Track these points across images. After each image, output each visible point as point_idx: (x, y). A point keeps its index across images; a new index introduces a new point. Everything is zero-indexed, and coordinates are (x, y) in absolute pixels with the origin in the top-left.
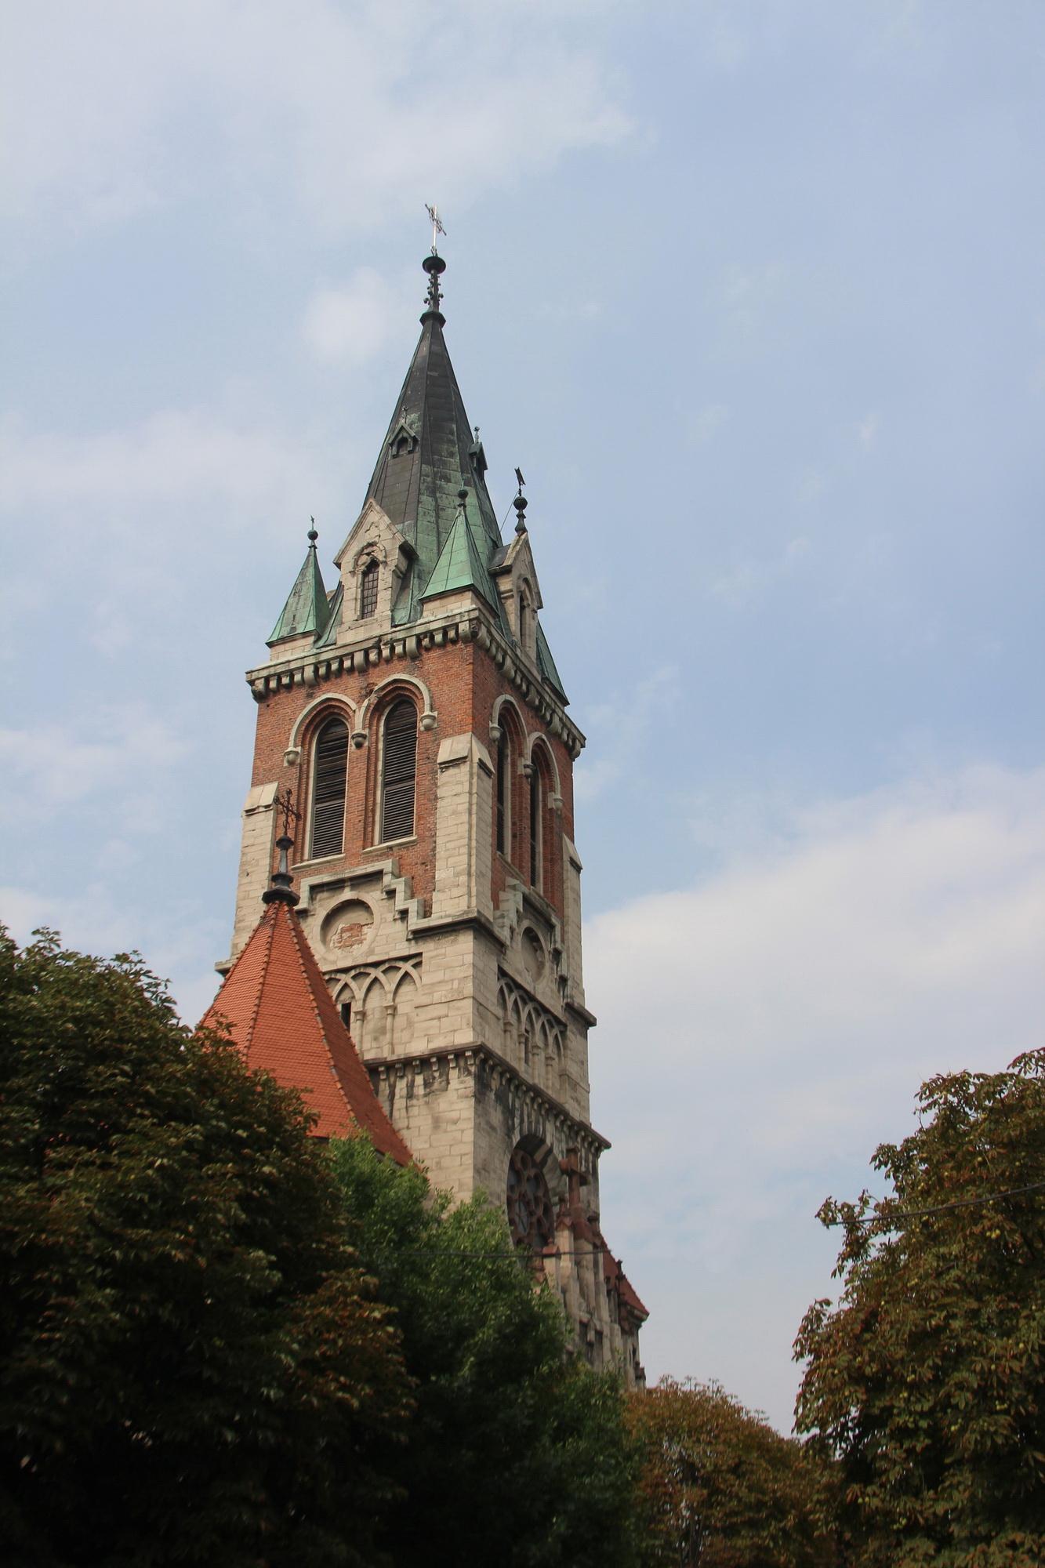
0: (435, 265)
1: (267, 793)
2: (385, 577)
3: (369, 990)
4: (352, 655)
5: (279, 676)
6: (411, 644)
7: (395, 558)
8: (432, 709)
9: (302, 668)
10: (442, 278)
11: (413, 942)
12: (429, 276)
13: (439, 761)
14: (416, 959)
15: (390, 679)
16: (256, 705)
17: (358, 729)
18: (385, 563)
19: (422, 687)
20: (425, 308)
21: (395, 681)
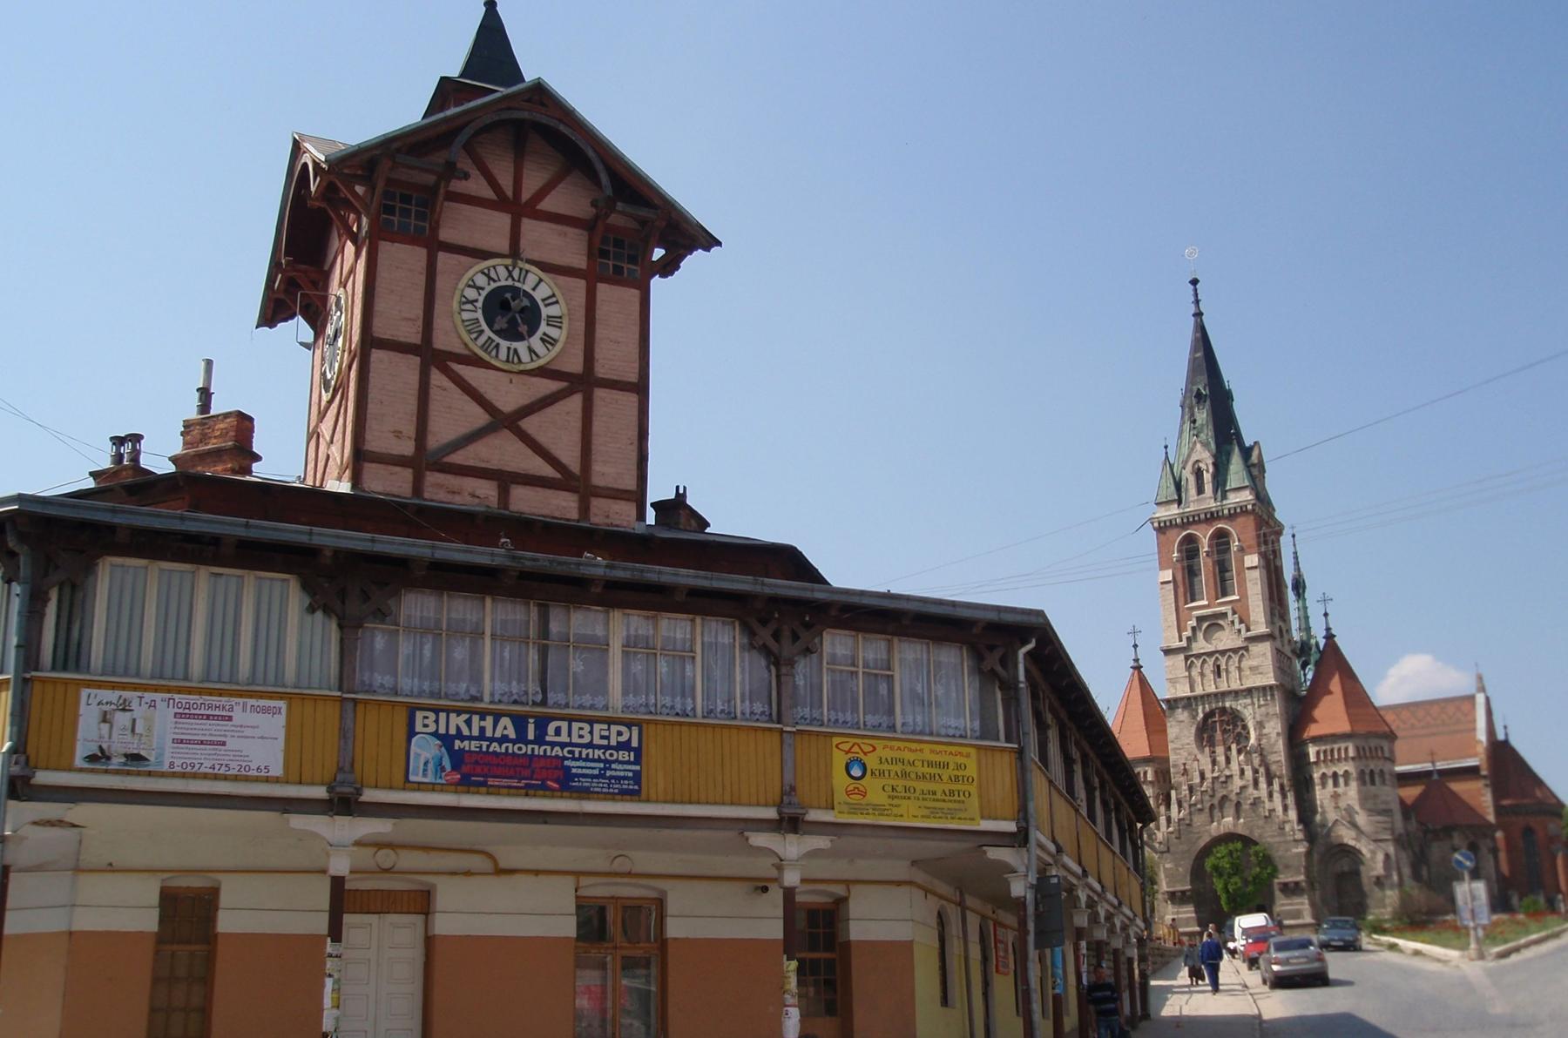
0: (1194, 282)
1: (1167, 575)
2: (1207, 477)
4: (1199, 515)
5: (1165, 522)
6: (1226, 512)
7: (1211, 470)
8: (1239, 541)
10: (1197, 286)
12: (1192, 287)
13: (1246, 565)
14: (1246, 649)
16: (1155, 533)
17: (1206, 549)
18: (1207, 471)
20: (1193, 309)
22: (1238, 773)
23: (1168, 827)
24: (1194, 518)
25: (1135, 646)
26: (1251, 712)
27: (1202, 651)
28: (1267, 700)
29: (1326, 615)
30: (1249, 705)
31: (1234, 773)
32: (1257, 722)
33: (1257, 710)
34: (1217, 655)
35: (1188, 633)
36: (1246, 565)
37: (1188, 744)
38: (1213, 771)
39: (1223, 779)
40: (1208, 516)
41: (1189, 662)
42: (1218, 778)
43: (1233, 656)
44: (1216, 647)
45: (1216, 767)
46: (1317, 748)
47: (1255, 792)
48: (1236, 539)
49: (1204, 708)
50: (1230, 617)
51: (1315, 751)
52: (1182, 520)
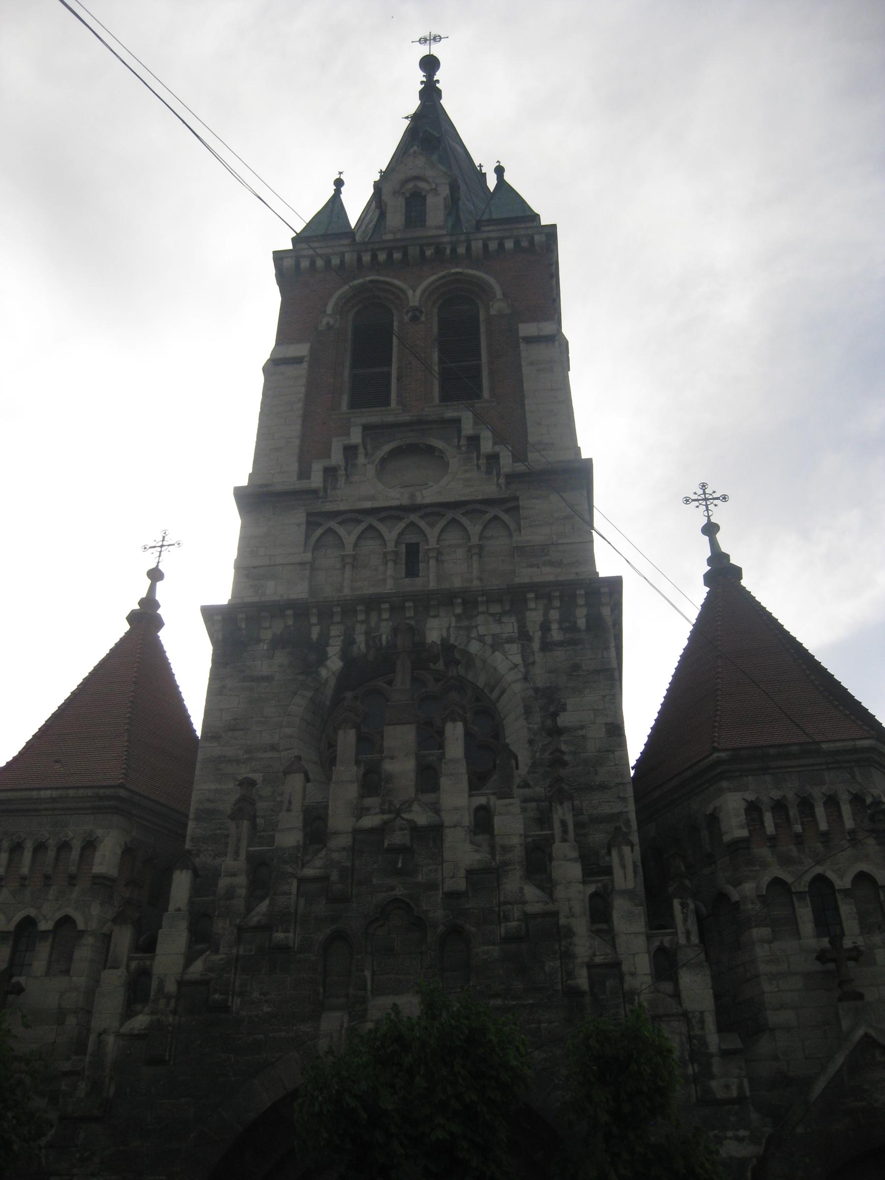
0: (430, 64)
3: (442, 532)
6: (477, 246)
7: (445, 191)
9: (343, 254)
11: (503, 486)
14: (511, 504)
15: (453, 271)
19: (492, 281)
21: (457, 273)
22: (467, 820)
23: (128, 1013)
24: (390, 256)
25: (155, 575)
26: (518, 659)
27: (368, 505)
28: (574, 628)
29: (710, 529)
30: (510, 641)
31: (448, 819)
32: (536, 690)
33: (538, 657)
34: (414, 517)
35: (337, 458)
36: (521, 334)
37: (273, 748)
38: (361, 811)
39: (398, 838)
40: (429, 252)
41: (319, 531)
42: (381, 831)
43: (465, 521)
44: (412, 496)
45: (370, 801)
46: (751, 797)
47: (531, 892)
48: (499, 294)
49: (349, 641)
50: (468, 427)
51: (743, 805)
52: (359, 259)
